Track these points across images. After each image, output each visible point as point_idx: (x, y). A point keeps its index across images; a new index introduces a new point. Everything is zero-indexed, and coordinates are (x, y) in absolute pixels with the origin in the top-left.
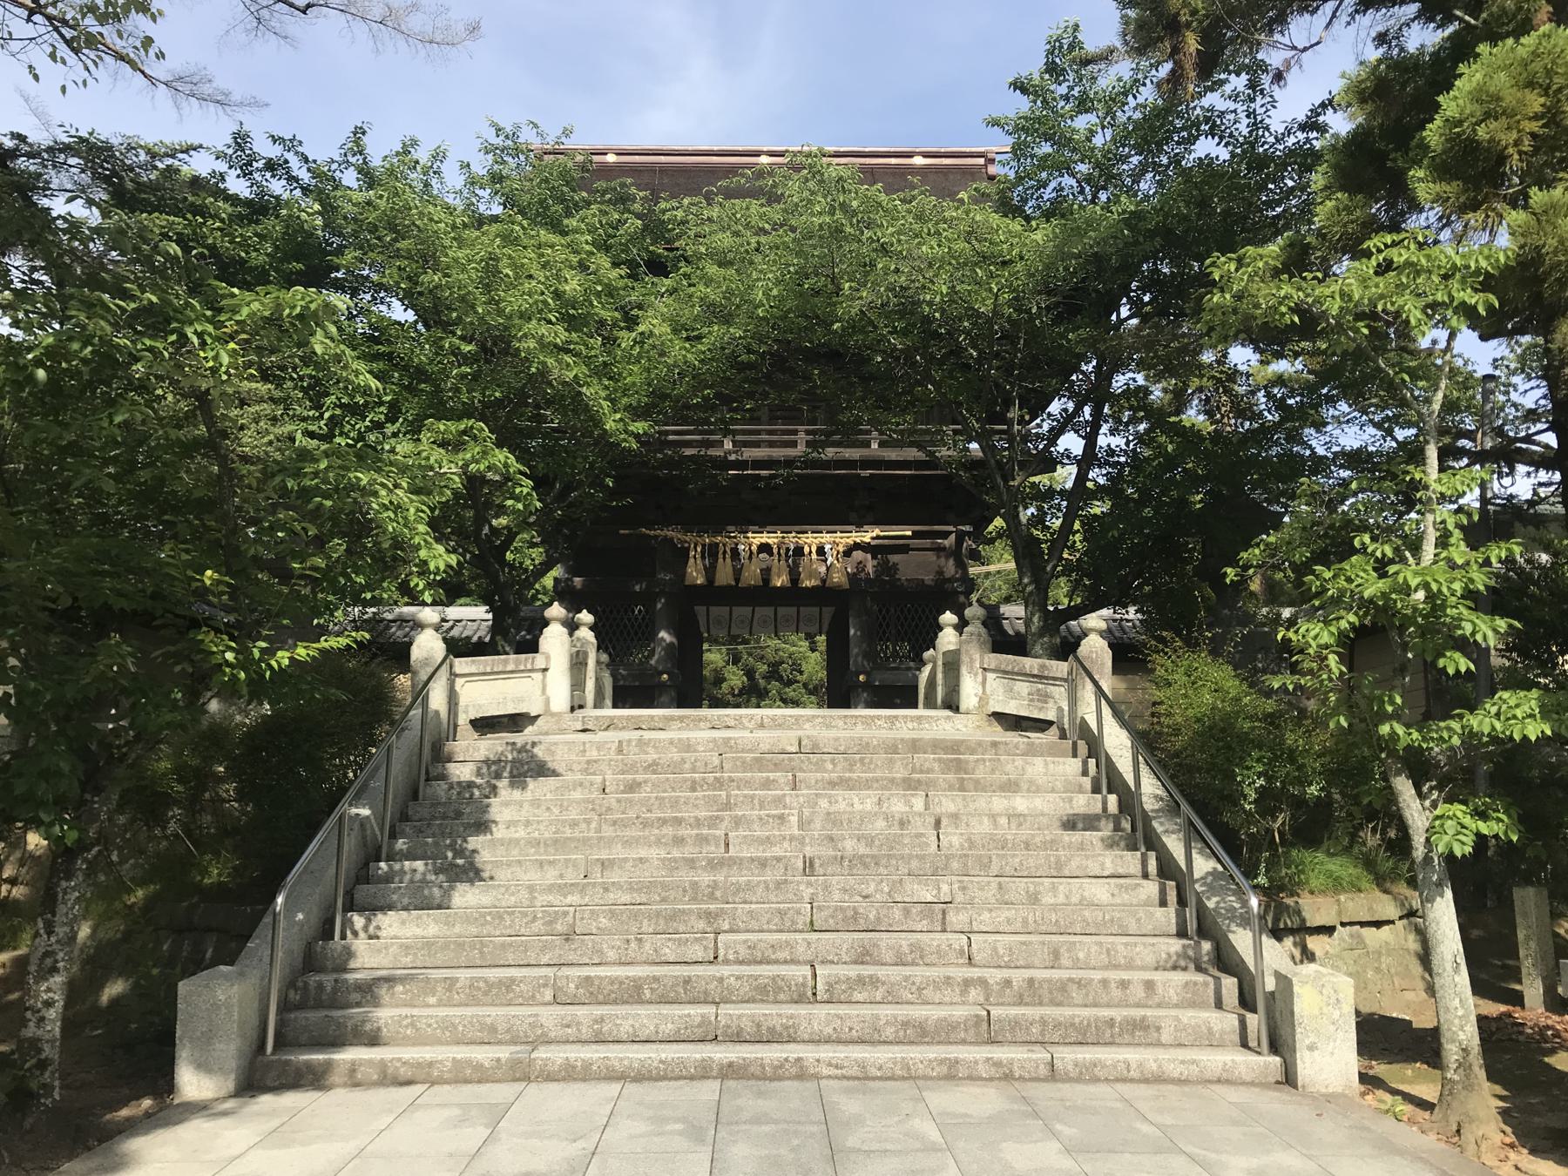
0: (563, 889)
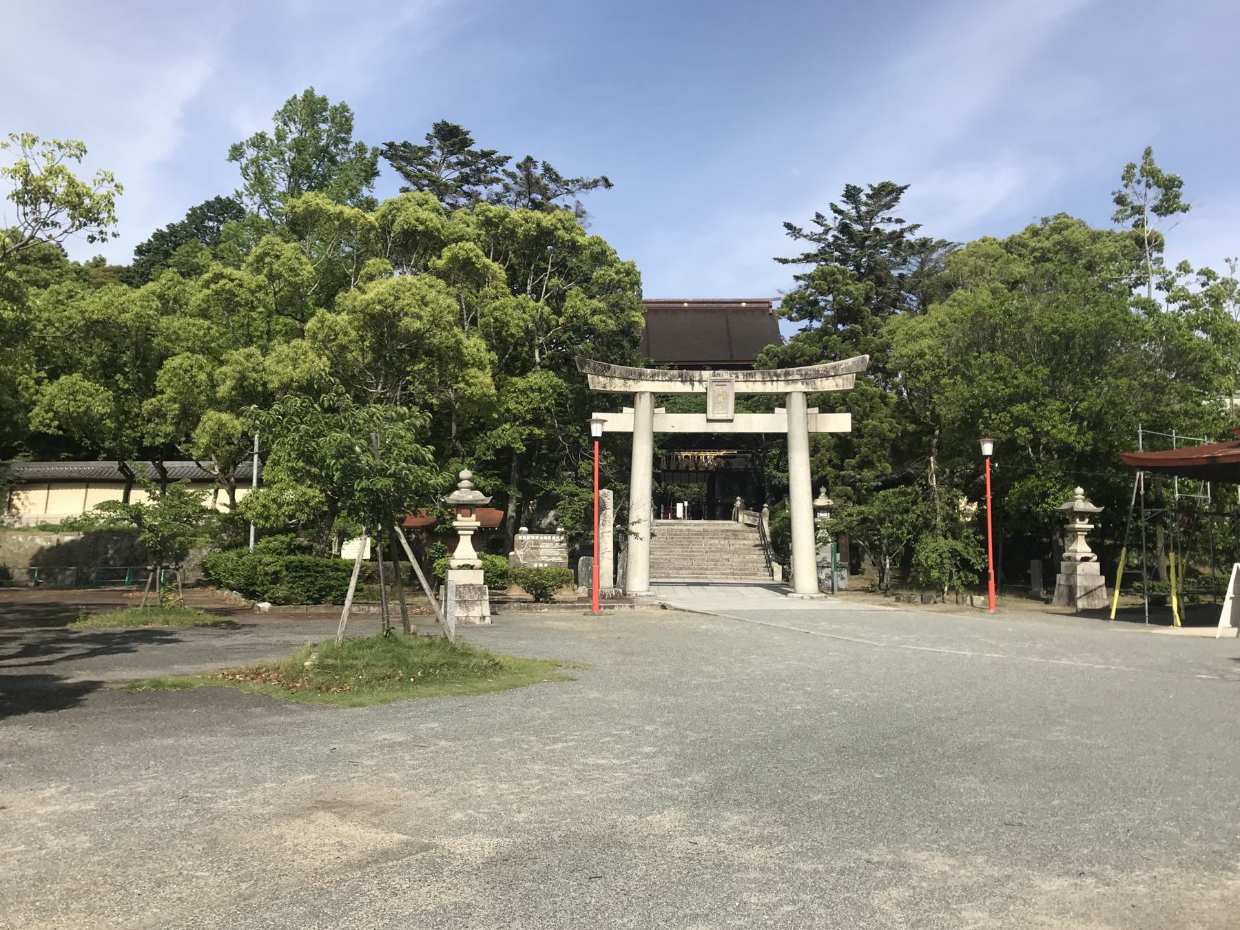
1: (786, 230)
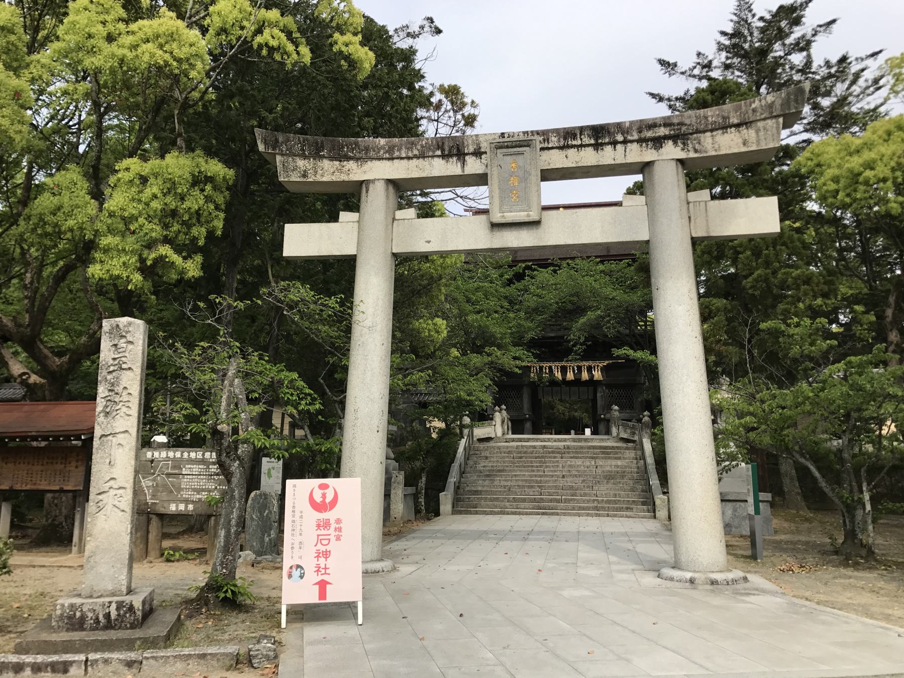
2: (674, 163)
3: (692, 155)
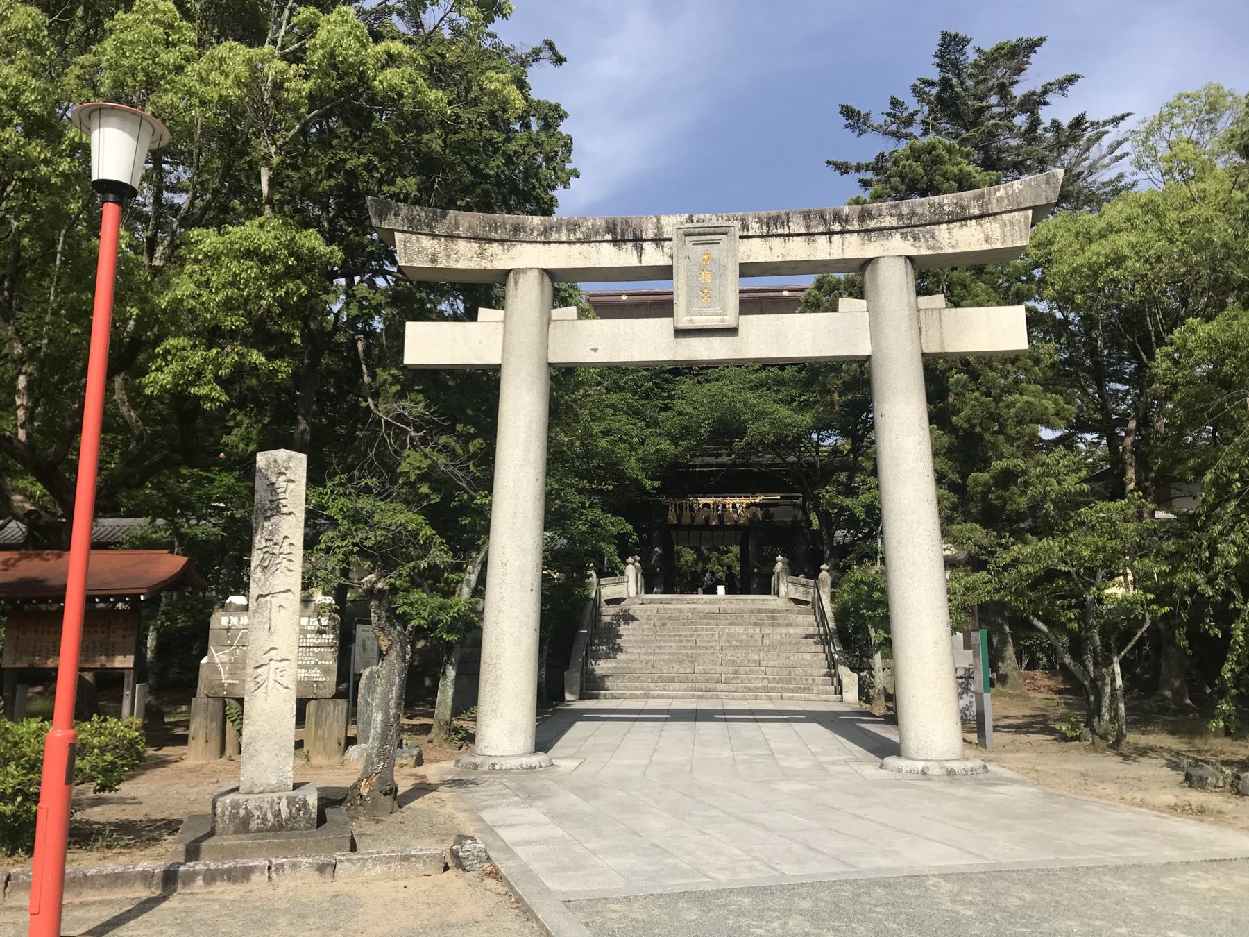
0: (649, 654)
1: (843, 120)
2: (902, 261)
3: (924, 252)
